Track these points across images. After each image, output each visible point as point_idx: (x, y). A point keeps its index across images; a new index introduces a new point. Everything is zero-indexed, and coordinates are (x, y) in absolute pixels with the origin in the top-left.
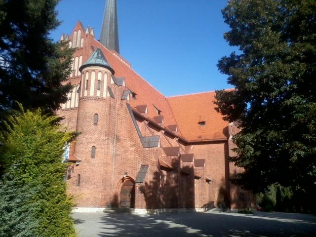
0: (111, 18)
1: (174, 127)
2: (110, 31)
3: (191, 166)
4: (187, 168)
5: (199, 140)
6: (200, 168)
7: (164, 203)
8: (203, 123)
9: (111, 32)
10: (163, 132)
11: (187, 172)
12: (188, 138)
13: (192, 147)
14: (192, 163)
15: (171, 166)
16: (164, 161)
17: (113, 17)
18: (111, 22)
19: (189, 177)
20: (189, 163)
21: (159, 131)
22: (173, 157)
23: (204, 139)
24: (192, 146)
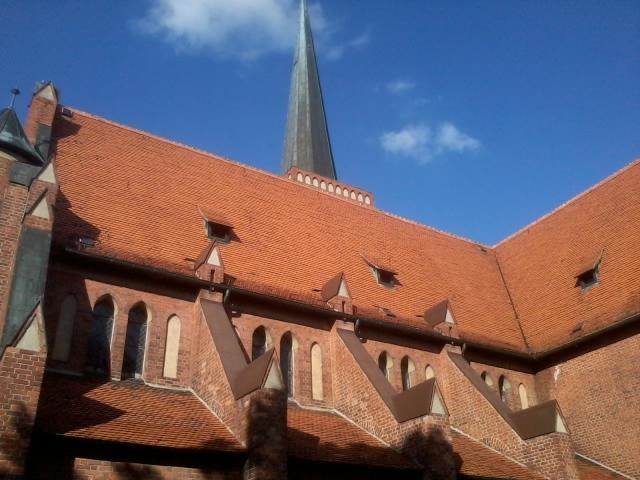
0: (302, 105)
1: (438, 312)
2: (299, 131)
3: (425, 431)
4: (415, 439)
5: (577, 337)
6: (541, 440)
8: (587, 278)
9: (303, 136)
12: (540, 341)
13: (557, 371)
14: (426, 419)
17: (305, 103)
18: (302, 114)
20: (418, 421)
21: (329, 330)
22: (247, 403)
23: (589, 330)
24: (557, 367)
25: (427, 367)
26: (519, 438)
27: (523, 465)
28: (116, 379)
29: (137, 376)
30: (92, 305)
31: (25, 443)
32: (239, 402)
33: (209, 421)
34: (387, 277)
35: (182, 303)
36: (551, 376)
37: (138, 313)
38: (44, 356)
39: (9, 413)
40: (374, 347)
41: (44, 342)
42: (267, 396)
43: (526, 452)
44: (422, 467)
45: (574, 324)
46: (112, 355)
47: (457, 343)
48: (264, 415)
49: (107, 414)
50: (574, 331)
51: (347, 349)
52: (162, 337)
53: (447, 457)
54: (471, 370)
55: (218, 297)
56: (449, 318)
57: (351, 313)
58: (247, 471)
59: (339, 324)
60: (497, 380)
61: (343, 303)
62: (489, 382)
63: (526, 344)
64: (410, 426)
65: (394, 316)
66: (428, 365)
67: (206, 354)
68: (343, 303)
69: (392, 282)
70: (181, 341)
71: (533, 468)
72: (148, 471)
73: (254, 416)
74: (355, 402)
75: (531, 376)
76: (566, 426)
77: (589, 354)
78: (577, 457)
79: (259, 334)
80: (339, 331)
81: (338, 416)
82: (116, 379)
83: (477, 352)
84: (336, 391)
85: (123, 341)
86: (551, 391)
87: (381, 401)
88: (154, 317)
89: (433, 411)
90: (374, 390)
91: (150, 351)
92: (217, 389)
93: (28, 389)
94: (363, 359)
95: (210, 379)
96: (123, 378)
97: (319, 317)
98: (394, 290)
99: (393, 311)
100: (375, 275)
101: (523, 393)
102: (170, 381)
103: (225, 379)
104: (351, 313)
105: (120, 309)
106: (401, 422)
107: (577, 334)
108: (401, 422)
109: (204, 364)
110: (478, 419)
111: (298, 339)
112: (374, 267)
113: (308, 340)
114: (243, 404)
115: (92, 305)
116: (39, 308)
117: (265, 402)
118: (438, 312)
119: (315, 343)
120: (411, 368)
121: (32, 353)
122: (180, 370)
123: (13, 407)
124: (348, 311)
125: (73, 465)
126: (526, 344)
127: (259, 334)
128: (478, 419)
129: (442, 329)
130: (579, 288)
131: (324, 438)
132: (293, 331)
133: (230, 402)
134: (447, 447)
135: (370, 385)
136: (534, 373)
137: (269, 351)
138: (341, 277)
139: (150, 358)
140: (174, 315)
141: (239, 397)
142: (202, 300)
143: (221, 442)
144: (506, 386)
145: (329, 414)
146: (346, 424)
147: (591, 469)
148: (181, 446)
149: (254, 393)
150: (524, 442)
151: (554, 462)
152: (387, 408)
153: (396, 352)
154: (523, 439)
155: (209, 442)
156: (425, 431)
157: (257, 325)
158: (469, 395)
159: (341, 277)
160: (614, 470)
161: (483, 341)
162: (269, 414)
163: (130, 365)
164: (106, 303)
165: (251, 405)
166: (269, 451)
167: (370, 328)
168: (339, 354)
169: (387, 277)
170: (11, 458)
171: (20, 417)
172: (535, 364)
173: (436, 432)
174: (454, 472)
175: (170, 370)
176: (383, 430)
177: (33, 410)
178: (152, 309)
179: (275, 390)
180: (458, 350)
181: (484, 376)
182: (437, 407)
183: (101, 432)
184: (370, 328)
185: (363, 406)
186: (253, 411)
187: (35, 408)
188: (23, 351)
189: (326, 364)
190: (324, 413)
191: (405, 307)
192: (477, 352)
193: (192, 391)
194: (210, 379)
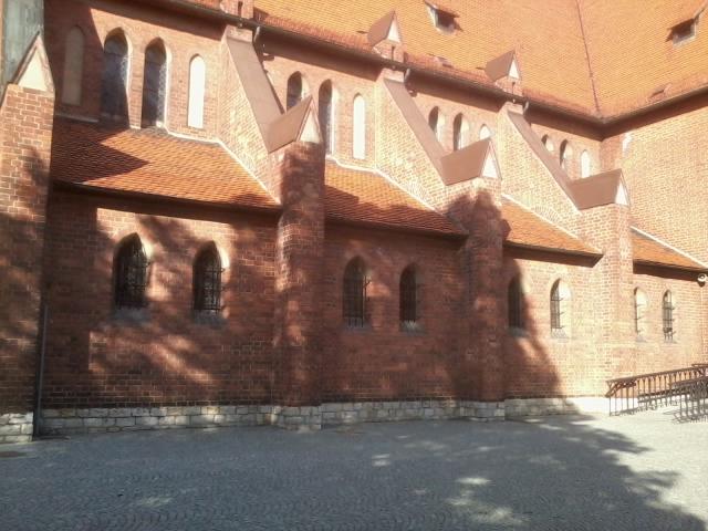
1: (501, 65)
3: (473, 195)
4: (461, 204)
5: (658, 100)
6: (598, 211)
7: (200, 376)
8: (683, 30)
10: (399, 77)
11: (462, 230)
13: (628, 138)
15: (277, 200)
16: (261, 183)
19: (469, 244)
20: (467, 184)
21: (375, 80)
22: (281, 157)
23: (672, 93)
25: (479, 124)
26: (575, 209)
27: (574, 236)
28: (135, 125)
29: (159, 124)
30: (102, 41)
31: (43, 191)
32: (273, 155)
33: (244, 178)
34: (446, 19)
35: (205, 41)
36: (619, 142)
37: (155, 52)
38: (52, 96)
39: (21, 158)
40: (425, 102)
41: (50, 80)
42: (303, 150)
43: (581, 222)
44: (467, 232)
45: (653, 87)
46: (129, 100)
47: (520, 101)
48: (300, 170)
49: (128, 164)
50: (655, 94)
51: (393, 103)
52: (184, 80)
53: (494, 223)
54: (532, 132)
55: (247, 36)
56: (514, 72)
57: (401, 61)
58: (281, 228)
59: (387, 73)
60: (558, 146)
61: (393, 48)
62: (551, 147)
63: (597, 107)
64: (457, 189)
65: (450, 67)
66: (484, 125)
67: (235, 102)
68: (393, 48)
69: (452, 26)
70: (206, 87)
71: (584, 239)
72: (174, 223)
73: (289, 171)
74: (400, 162)
75: (597, 143)
76: (628, 198)
77: (667, 121)
78: (633, 231)
79: (295, 81)
80: (387, 81)
81: (380, 176)
82: (135, 125)
83: (541, 113)
84: (379, 149)
85: (141, 84)
86: (616, 160)
87: (428, 161)
88: (174, 57)
89: (484, 174)
90: (422, 151)
91: (172, 96)
92: (248, 140)
93: (38, 132)
94: (411, 115)
95: (239, 130)
96: (143, 126)
97: (364, 64)
98: (453, 35)
99: (450, 61)
100: (433, 17)
101: (585, 157)
102: (195, 131)
103: (256, 131)
104: (401, 61)
105: (135, 46)
106: (449, 183)
107: (656, 98)
108: (449, 183)
109: (233, 113)
110: (532, 186)
111: (339, 89)
112: (432, 8)
113: (350, 90)
114: (277, 157)
115: (102, 41)
116: (39, 42)
117: (301, 156)
118: (501, 65)
119: (358, 94)
120: (464, 127)
121: (38, 92)
122: (206, 119)
123: (24, 152)
124: (398, 58)
125: (96, 216)
126: (597, 107)
127: (295, 81)
128: (532, 186)
129: (503, 85)
130: (671, 42)
131: (364, 198)
132: (333, 80)
133: (263, 154)
134: (495, 212)
135: (417, 144)
136: (601, 141)
137: (306, 99)
138: (392, 17)
139: (172, 104)
140: (197, 55)
141: (272, 149)
142: (228, 38)
143: (253, 197)
144: (568, 152)
145: (371, 174)
146: (388, 185)
147: (643, 243)
148: (210, 199)
149: (289, 146)
150: (579, 212)
151: (608, 234)
152: (434, 170)
153: (449, 108)
154: (580, 209)
155: (240, 197)
156: (473, 195)
157: (292, 71)
158: (526, 159)
159: (392, 17)
160: (668, 246)
161: (548, 101)
162: (305, 170)
163: (151, 112)
164: (117, 38)
165: (285, 158)
166: (303, 207)
167: (422, 79)
168: (385, 107)
169: (446, 19)
170: (29, 206)
171: (33, 164)
172: (602, 130)
173: (484, 196)
174: (500, 240)
175: (196, 119)
176: (429, 193)
177: (46, 156)
178: (171, 47)
179: (312, 144)
180: (519, 110)
181: (544, 139)
182: (489, 169)
183: (121, 182)
184: (422, 79)
185: (408, 166)
186: (288, 165)
187: (49, 154)
188: (26, 90)
189: (369, 119)
190: (366, 173)
191: (463, 55)
192: (541, 113)
193: (221, 143)
194: (239, 130)
